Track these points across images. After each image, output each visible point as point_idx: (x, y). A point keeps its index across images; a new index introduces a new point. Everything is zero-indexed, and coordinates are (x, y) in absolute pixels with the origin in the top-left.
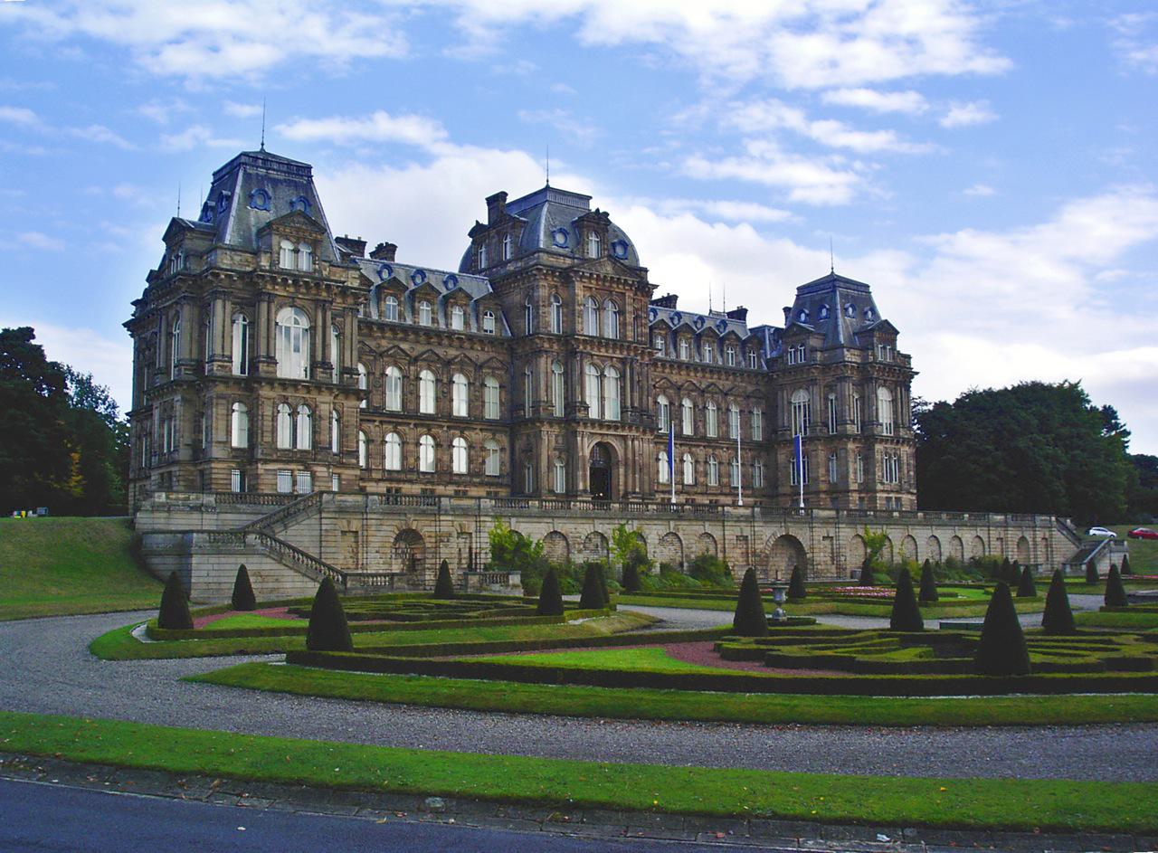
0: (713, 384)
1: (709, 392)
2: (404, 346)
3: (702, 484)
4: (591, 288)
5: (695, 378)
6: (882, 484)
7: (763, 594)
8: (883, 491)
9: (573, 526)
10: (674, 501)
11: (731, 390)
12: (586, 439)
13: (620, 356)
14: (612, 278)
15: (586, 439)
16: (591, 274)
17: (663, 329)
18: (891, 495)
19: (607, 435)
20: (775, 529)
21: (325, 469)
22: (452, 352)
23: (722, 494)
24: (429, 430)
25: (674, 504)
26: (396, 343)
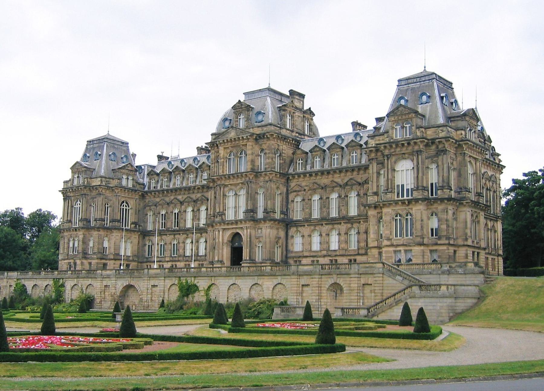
0: (351, 179)
1: (186, 202)
2: (180, 197)
3: (343, 249)
4: (228, 147)
5: (339, 179)
6: (389, 239)
7: (134, 317)
8: (392, 245)
9: (41, 282)
10: (193, 266)
11: (365, 181)
12: (221, 233)
13: (241, 182)
14: (235, 139)
15: (221, 233)
16: (224, 141)
17: (317, 151)
18: (398, 249)
19: (236, 228)
20: (123, 281)
21: (79, 261)
22: (199, 195)
23: (358, 254)
24: (188, 235)
25: (192, 268)
26: (176, 197)
